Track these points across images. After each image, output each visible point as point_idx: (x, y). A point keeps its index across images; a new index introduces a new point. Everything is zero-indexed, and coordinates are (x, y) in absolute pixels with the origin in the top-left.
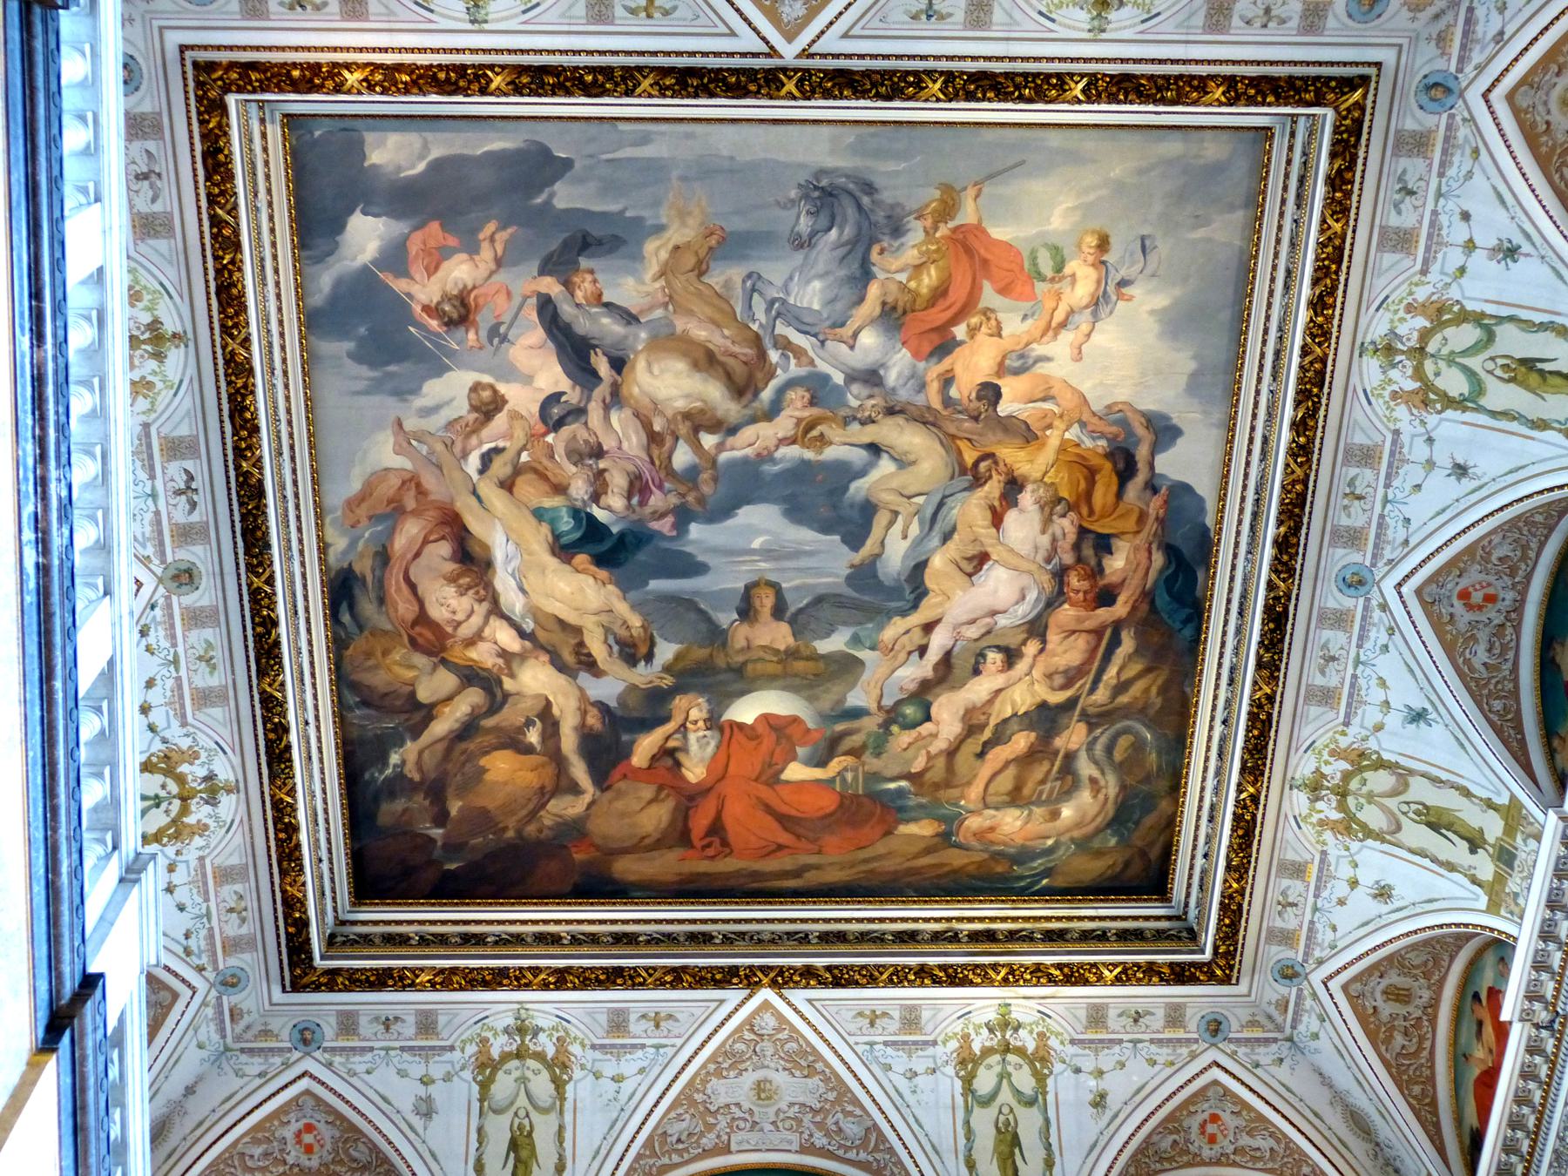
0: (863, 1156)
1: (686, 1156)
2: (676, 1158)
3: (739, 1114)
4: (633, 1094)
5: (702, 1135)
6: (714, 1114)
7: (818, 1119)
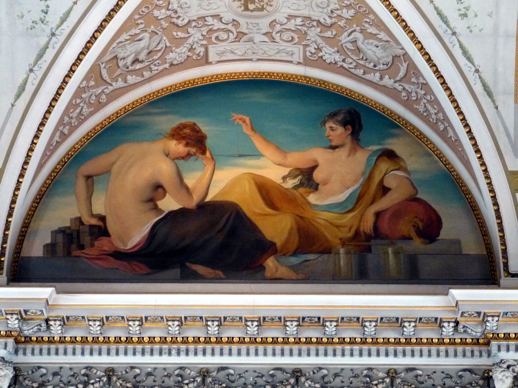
0: (388, 81)
1: (147, 74)
2: (132, 79)
3: (217, 25)
4: (68, 14)
5: (167, 49)
6: (184, 28)
7: (329, 34)
